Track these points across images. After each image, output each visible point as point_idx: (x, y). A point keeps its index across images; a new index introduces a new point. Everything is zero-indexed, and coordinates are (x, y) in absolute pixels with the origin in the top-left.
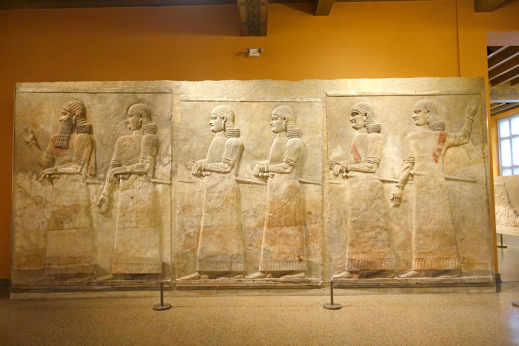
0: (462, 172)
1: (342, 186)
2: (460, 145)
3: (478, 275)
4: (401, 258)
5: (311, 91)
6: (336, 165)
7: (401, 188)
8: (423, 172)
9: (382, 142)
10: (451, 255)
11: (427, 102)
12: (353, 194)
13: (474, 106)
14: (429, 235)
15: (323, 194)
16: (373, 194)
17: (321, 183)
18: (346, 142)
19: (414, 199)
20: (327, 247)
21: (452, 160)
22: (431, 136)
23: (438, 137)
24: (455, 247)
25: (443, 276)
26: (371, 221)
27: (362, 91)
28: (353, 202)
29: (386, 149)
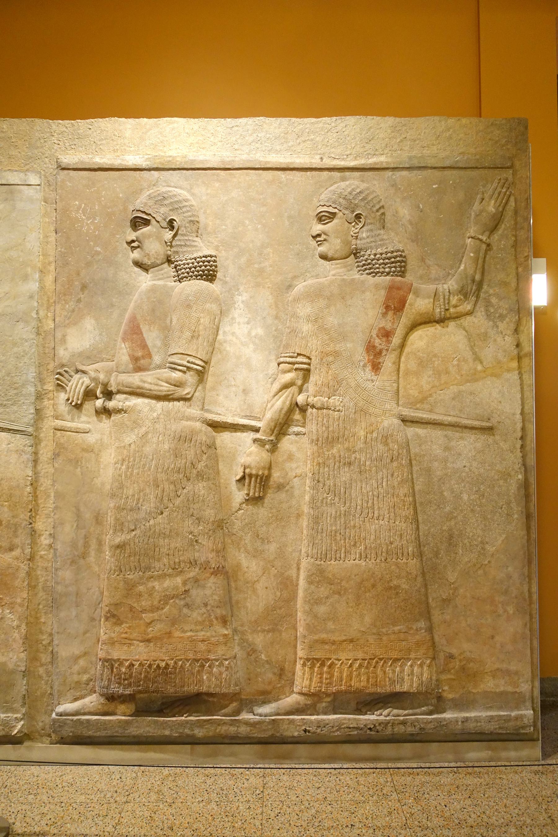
0: (453, 399)
1: (91, 439)
2: (449, 319)
3: (490, 708)
4: (263, 657)
5: (14, 152)
6: (77, 376)
7: (267, 447)
8: (334, 401)
9: (214, 307)
10: (409, 650)
11: (353, 190)
12: (122, 465)
13: (493, 202)
14: (346, 589)
15: (36, 462)
16: (180, 463)
17: (30, 429)
18: (112, 306)
19: (308, 481)
20: (43, 620)
21: (422, 364)
22: (363, 292)
23: (383, 293)
24: (422, 624)
25: (386, 712)
26: (172, 546)
27: (163, 154)
28: (121, 487)
29: (227, 328)
